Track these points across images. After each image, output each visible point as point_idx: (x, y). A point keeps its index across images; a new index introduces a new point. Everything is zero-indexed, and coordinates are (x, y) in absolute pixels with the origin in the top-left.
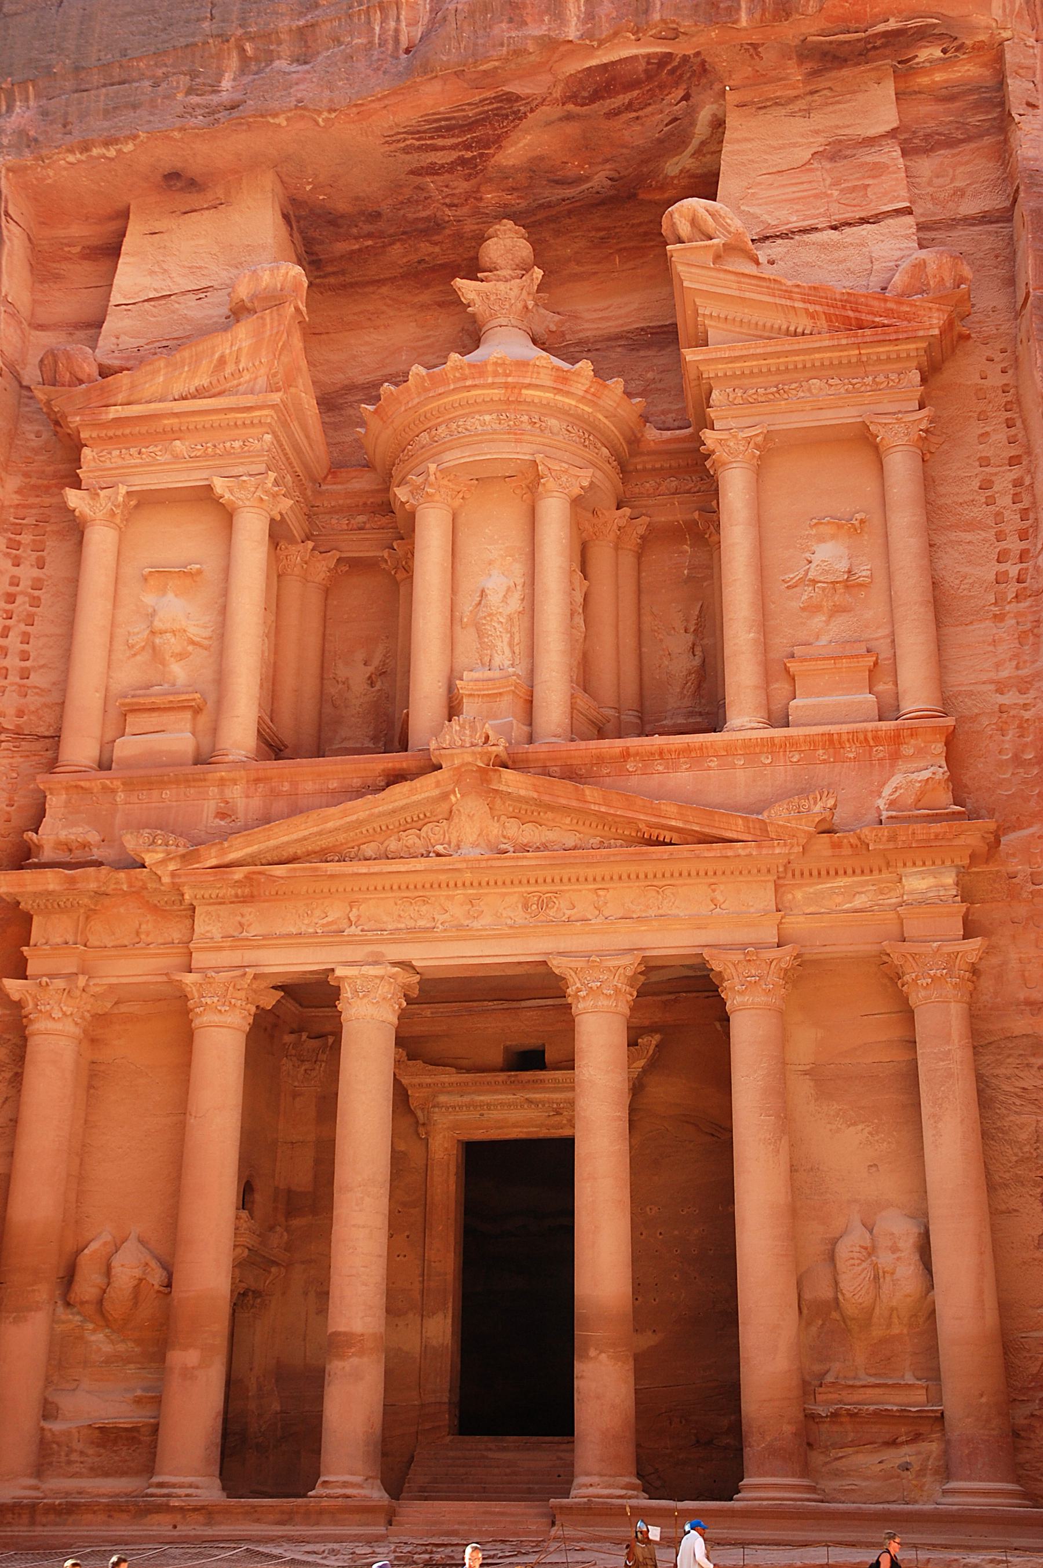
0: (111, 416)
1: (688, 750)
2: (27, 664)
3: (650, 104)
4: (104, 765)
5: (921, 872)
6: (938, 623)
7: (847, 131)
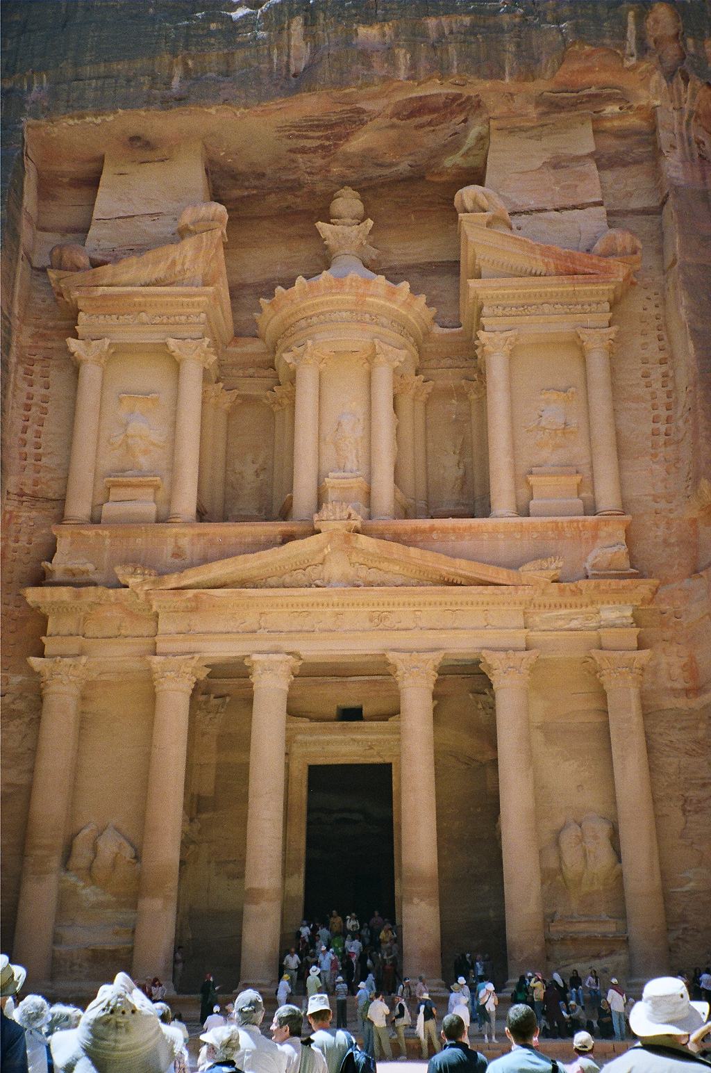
0: (99, 294)
1: (470, 527)
2: (40, 451)
3: (442, 123)
4: (95, 520)
5: (611, 609)
6: (619, 458)
7: (563, 151)
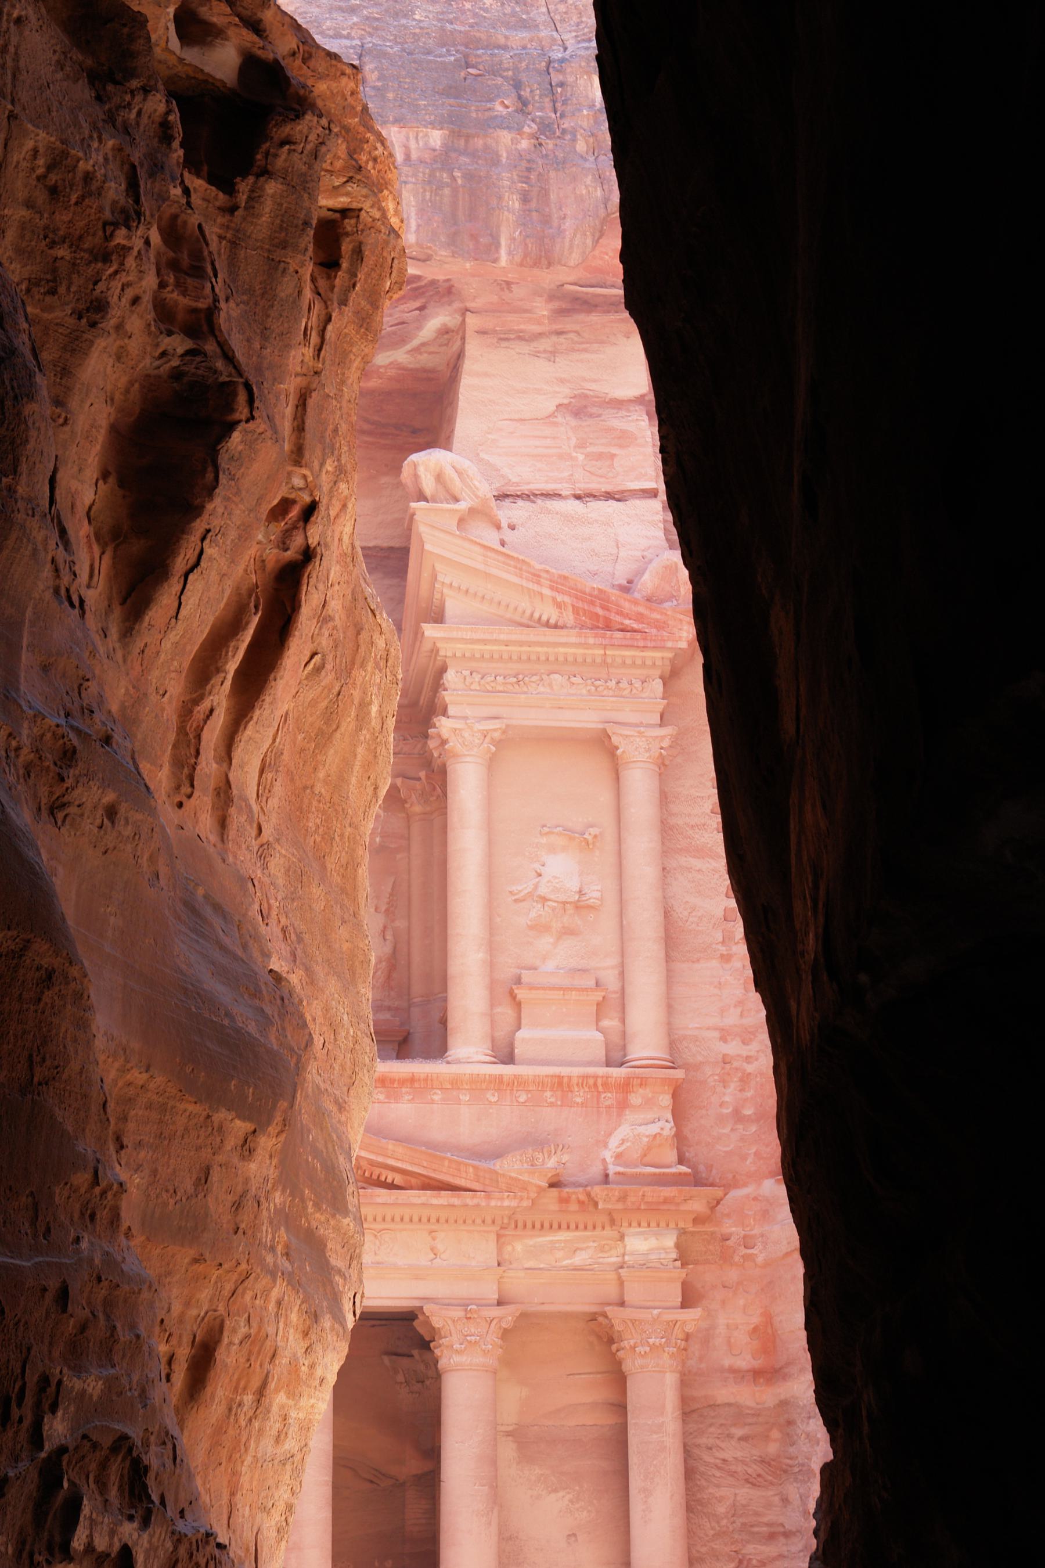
1: (412, 1080)
7: (594, 386)
